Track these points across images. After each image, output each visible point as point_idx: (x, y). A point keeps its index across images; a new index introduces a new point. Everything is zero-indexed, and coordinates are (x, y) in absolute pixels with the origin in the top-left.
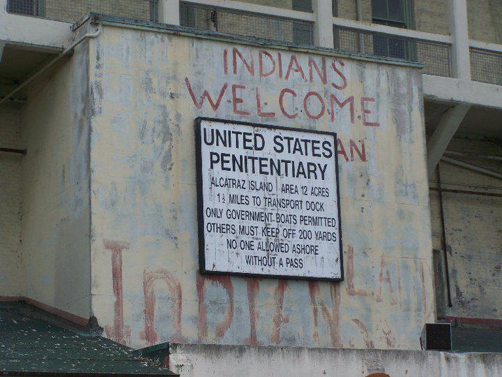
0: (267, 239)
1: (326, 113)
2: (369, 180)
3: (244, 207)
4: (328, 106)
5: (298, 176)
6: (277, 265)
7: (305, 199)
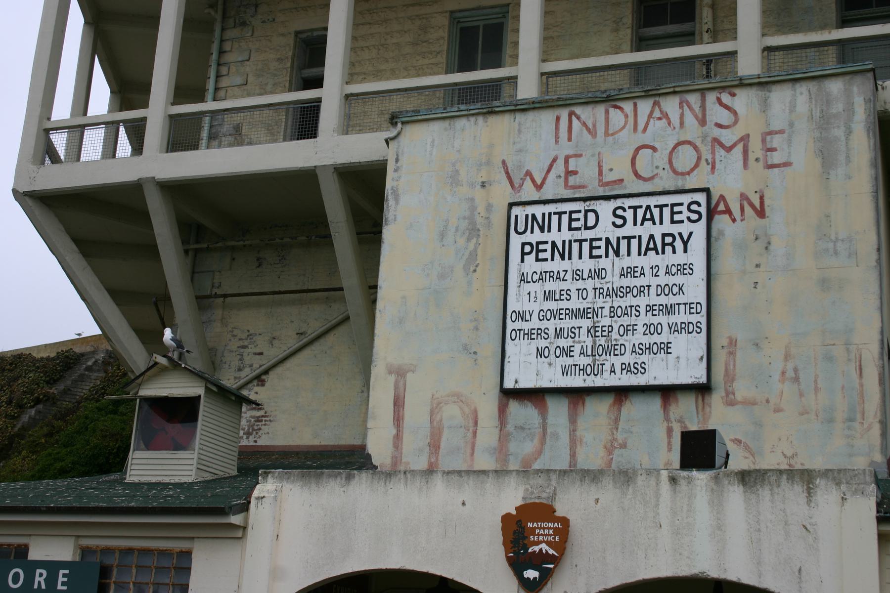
1: (703, 162)
2: (769, 243)
4: (706, 154)
5: (645, 254)
6: (606, 374)
7: (654, 281)
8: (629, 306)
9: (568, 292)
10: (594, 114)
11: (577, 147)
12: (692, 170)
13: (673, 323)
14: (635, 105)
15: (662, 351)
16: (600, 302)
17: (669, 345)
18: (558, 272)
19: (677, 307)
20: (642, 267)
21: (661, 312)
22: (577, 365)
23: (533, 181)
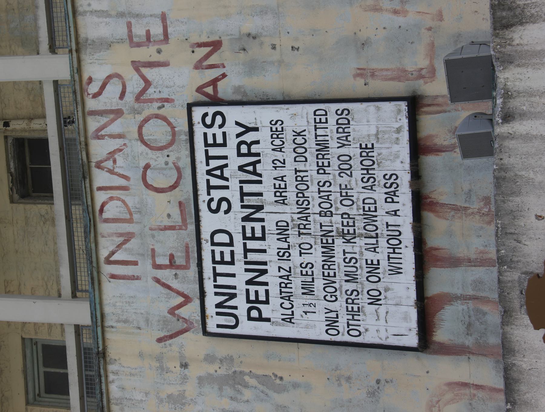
0: (361, 235)
1: (162, 112)
2: (249, 35)
3: (317, 271)
5: (260, 175)
7: (290, 165)
8: (319, 194)
9: (304, 265)
10: (109, 236)
11: (143, 255)
12: (169, 124)
13: (338, 142)
14: (100, 189)
15: (370, 154)
16: (314, 228)
17: (364, 146)
18: (281, 277)
19: (319, 138)
20: (275, 179)
21: (326, 157)
22: (389, 256)
23: (180, 306)
